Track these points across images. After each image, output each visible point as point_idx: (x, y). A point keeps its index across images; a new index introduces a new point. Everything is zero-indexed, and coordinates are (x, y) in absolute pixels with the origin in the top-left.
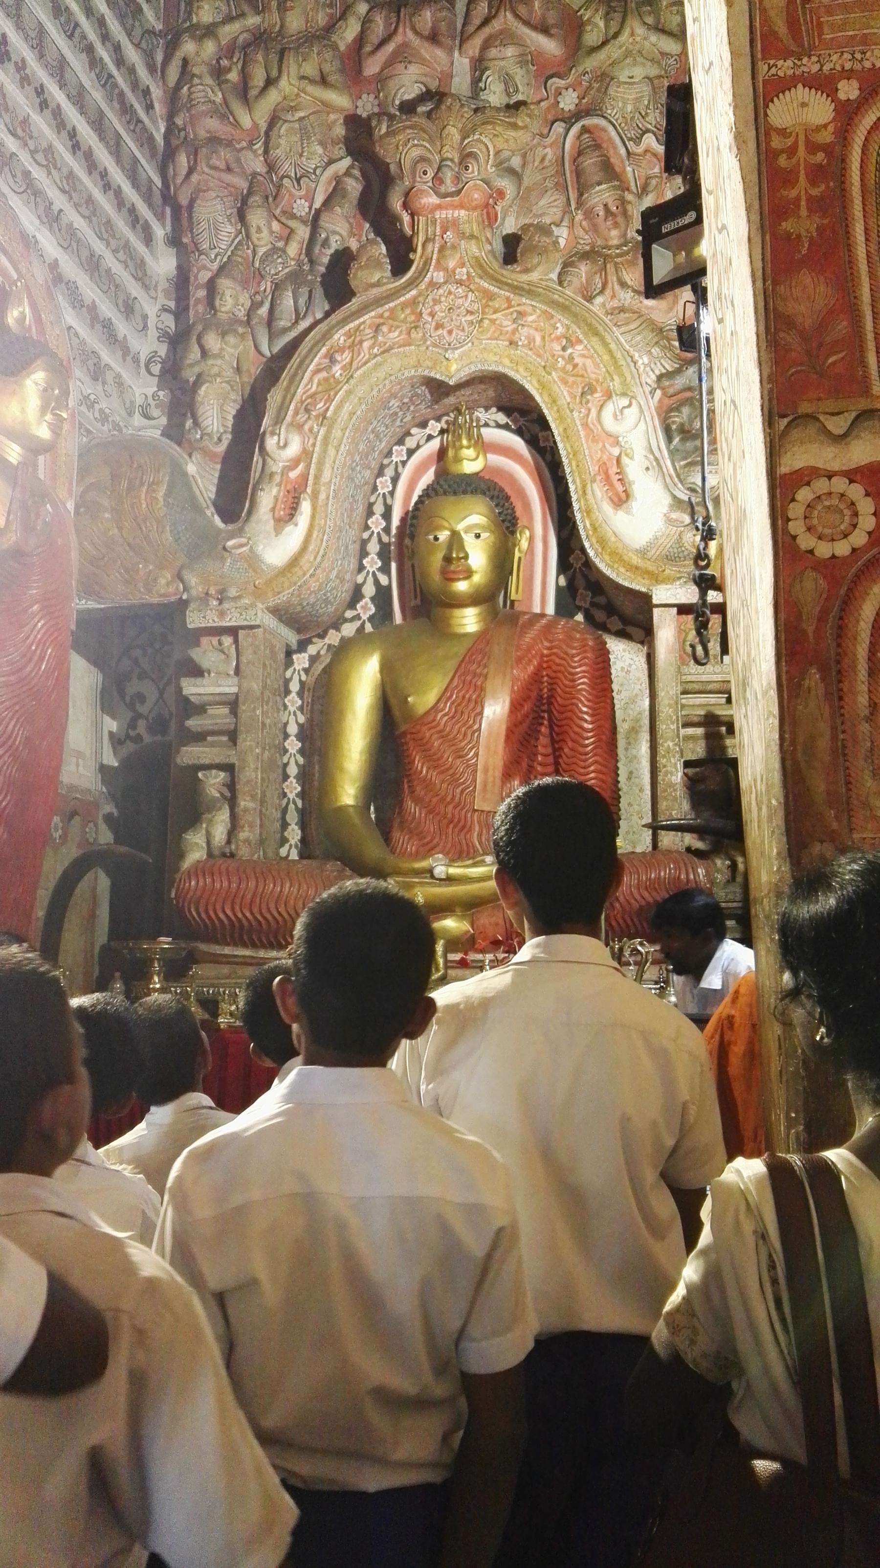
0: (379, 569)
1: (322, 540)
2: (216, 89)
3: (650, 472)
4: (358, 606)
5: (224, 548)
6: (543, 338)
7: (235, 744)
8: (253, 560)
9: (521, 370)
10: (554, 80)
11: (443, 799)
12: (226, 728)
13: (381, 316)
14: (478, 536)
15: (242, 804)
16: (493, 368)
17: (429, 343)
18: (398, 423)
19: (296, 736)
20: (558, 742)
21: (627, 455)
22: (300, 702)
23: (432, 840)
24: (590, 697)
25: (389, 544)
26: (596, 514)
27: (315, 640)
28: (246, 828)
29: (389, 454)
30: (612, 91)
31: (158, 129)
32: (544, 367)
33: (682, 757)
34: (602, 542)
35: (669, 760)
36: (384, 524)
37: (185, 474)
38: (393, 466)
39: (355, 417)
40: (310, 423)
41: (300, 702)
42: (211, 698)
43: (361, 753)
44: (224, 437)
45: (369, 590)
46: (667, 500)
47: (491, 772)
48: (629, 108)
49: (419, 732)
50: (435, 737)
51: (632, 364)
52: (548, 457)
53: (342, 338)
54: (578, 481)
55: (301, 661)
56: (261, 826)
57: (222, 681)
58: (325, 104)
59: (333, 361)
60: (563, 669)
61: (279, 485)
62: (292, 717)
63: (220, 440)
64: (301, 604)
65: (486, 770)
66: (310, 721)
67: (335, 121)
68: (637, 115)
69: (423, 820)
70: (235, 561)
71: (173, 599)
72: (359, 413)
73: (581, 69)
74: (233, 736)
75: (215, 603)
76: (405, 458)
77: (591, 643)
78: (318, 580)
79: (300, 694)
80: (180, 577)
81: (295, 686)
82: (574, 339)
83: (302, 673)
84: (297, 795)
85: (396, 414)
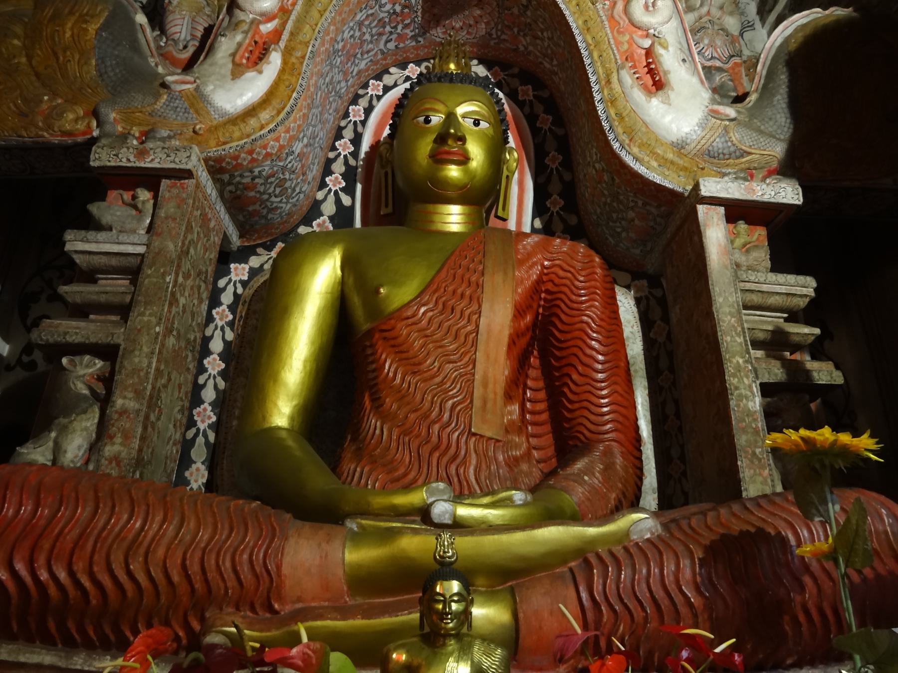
0: (342, 189)
3: (687, 65)
4: (314, 223)
5: (164, 85)
7: (126, 322)
11: (426, 416)
12: (116, 299)
14: (477, 123)
15: (119, 402)
18: (382, 46)
19: (219, 355)
20: (558, 369)
21: (660, 44)
22: (231, 317)
23: (405, 475)
24: (603, 316)
25: (356, 168)
26: (621, 103)
27: (260, 250)
28: (118, 440)
29: (365, 86)
33: (757, 377)
34: (631, 133)
35: (741, 380)
36: (352, 149)
37: (132, 22)
38: (367, 98)
41: (231, 317)
42: (104, 260)
43: (305, 361)
44: (191, 43)
45: (329, 208)
46: (706, 95)
47: (491, 386)
49: (393, 329)
50: (414, 335)
52: (527, 109)
54: (601, 70)
55: (239, 271)
56: (143, 439)
57: (123, 238)
60: (568, 283)
61: (246, 32)
62: (218, 332)
63: (185, 47)
64: (251, 171)
65: (485, 385)
66: (240, 337)
69: (394, 444)
70: (172, 99)
71: (80, 139)
74: (124, 311)
75: (135, 142)
76: (381, 93)
77: (597, 260)
78: (277, 140)
79: (232, 308)
80: (95, 114)
81: (227, 298)
83: (239, 285)
84: (210, 426)
85: (382, 23)
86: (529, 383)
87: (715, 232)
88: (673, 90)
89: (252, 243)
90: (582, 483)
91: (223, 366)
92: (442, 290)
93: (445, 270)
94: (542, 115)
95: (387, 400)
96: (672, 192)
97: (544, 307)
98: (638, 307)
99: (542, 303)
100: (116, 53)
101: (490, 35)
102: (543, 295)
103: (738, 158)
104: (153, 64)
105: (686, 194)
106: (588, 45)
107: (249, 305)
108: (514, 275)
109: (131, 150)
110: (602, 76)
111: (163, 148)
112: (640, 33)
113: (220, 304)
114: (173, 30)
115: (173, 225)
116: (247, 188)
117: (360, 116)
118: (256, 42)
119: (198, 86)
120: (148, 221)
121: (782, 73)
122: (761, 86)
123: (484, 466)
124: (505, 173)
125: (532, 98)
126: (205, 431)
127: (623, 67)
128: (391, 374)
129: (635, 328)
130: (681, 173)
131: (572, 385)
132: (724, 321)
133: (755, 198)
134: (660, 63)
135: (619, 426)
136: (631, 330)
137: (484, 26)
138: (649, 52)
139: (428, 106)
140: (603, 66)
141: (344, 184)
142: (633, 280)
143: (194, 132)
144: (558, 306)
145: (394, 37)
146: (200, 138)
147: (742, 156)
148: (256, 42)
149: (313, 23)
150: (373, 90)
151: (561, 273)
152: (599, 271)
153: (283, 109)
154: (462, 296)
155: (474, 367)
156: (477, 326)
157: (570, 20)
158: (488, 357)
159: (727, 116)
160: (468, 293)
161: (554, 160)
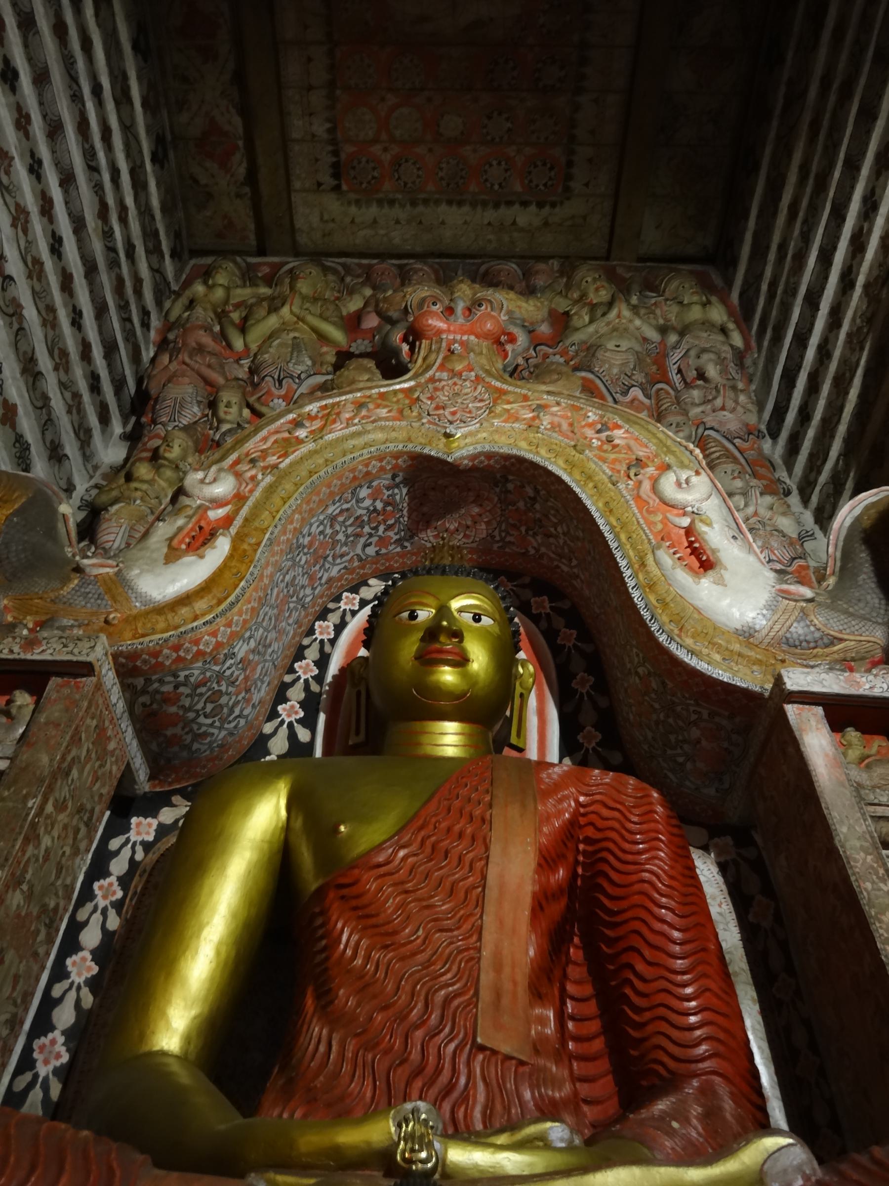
0: (298, 721)
1: (238, 585)
2: (216, 323)
5: (78, 569)
6: (571, 425)
8: (118, 586)
9: (543, 452)
10: (543, 347)
11: (403, 1017)
13: (369, 397)
14: (477, 618)
16: (505, 450)
17: (424, 421)
18: (359, 550)
19: (93, 952)
21: (701, 521)
22: (120, 894)
24: (672, 873)
25: (320, 694)
26: (661, 588)
29: (338, 599)
30: (600, 354)
31: (147, 349)
32: (575, 447)
34: (679, 620)
38: (339, 614)
39: (315, 477)
40: (253, 472)
41: (120, 894)
47: (507, 970)
48: (615, 371)
51: (688, 453)
53: (315, 410)
54: (631, 553)
55: (143, 829)
58: (323, 338)
59: (297, 424)
60: (617, 825)
62: (97, 917)
64: (176, 676)
65: (498, 967)
67: (326, 353)
68: (623, 376)
69: (346, 1068)
70: (84, 583)
72: (322, 473)
73: (568, 342)
75: (25, 632)
76: (357, 608)
77: (655, 795)
78: (214, 634)
79: (124, 881)
81: (118, 866)
82: (610, 425)
83: (139, 849)
84: (56, 1072)
85: (359, 522)
86: (570, 988)
87: (817, 741)
88: (726, 569)
89: (167, 789)
90: (671, 1133)
91: (95, 969)
92: (431, 827)
93: (435, 801)
94: (563, 630)
95: (342, 992)
96: (746, 693)
97: (584, 865)
98: (724, 876)
99: (581, 858)
100: (26, 538)
101: (493, 537)
102: (581, 847)
103: (827, 646)
104: (70, 555)
105: (767, 694)
106: (613, 527)
107: (150, 875)
108: (536, 808)
109: (18, 640)
110: (634, 559)
111: (61, 638)
112: (675, 511)
113: (108, 874)
114: (106, 538)
115: (54, 733)
116: (167, 700)
117: (329, 634)
118: (201, 528)
119: (120, 571)
120: (21, 731)
121: (862, 551)
122: (837, 569)
123: (498, 1107)
124: (518, 690)
125: (548, 611)
126: (46, 1079)
127: (659, 548)
128: (349, 952)
129: (724, 906)
130: (755, 668)
131: (636, 982)
132: (856, 861)
133: (861, 692)
134: (705, 541)
135: (721, 1049)
136: (718, 909)
137: (484, 526)
138: (689, 531)
139: (413, 600)
140: (634, 549)
141: (301, 714)
142: (711, 837)
143: (106, 622)
144: (605, 860)
145: (374, 540)
146: (111, 629)
147: (832, 644)
148: (201, 528)
149: (275, 509)
150: (346, 604)
151: (605, 812)
152: (659, 809)
153: (226, 598)
154: (461, 835)
155: (480, 939)
156: (484, 877)
157: (588, 503)
158: (501, 923)
159: (802, 596)
160: (469, 831)
161: (583, 683)
